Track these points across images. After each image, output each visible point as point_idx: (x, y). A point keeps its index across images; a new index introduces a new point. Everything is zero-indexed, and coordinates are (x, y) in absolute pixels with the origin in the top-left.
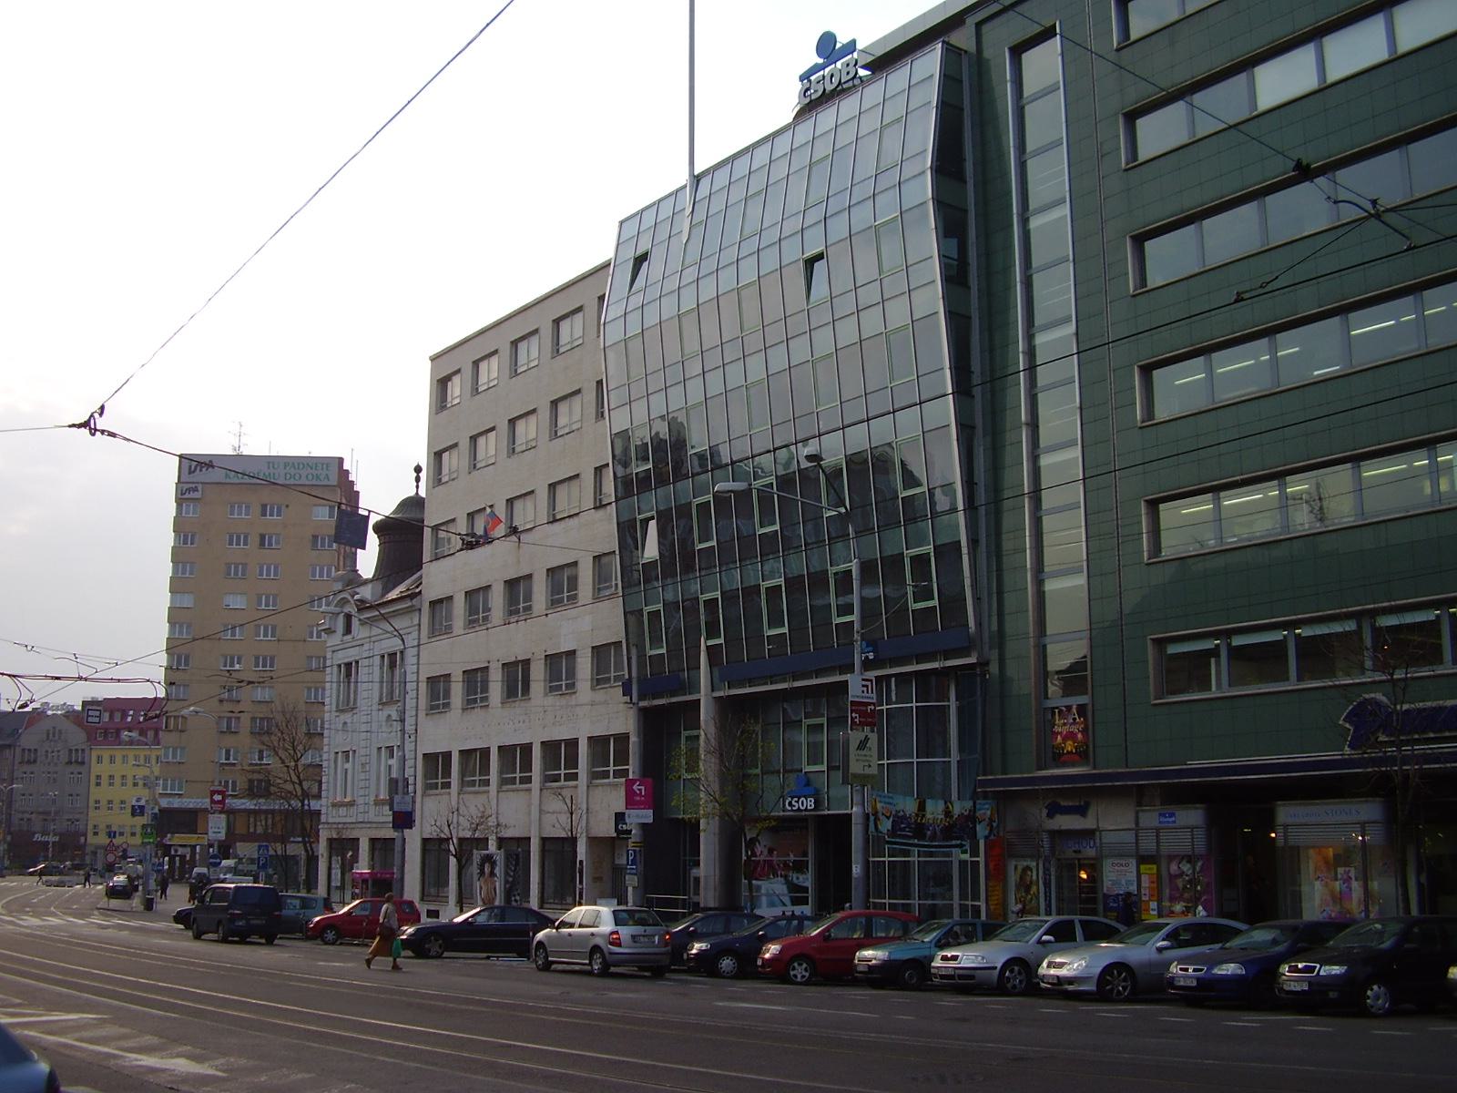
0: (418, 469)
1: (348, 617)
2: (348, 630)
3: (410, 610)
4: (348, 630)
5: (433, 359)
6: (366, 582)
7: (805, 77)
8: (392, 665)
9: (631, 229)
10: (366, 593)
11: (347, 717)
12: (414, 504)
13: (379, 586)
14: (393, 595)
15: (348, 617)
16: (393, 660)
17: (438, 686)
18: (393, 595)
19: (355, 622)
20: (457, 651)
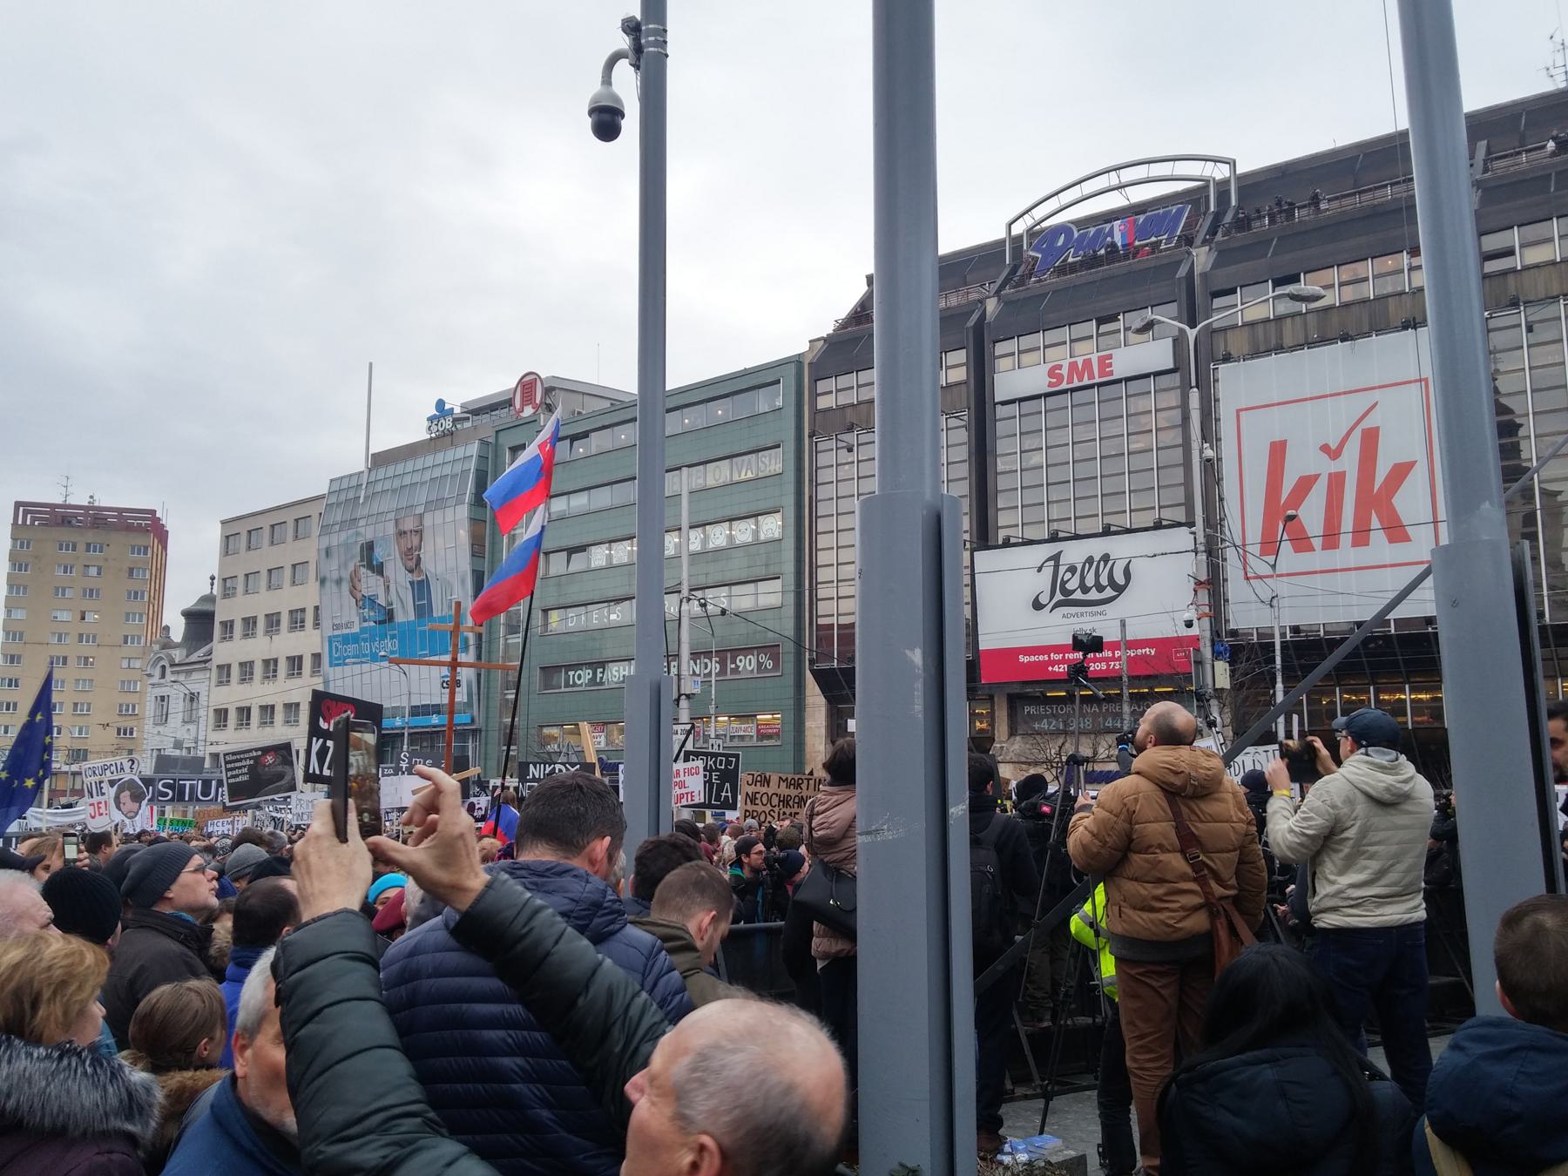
0: (213, 578)
1: (163, 667)
2: (163, 676)
3: (205, 669)
4: (163, 676)
5: (223, 523)
6: (177, 646)
7: (431, 419)
8: (192, 700)
9: (336, 487)
10: (178, 655)
11: (161, 729)
12: (209, 599)
13: (184, 652)
14: (194, 658)
15: (163, 667)
16: (193, 698)
17: (221, 715)
18: (194, 658)
19: (168, 670)
20: (234, 695)
